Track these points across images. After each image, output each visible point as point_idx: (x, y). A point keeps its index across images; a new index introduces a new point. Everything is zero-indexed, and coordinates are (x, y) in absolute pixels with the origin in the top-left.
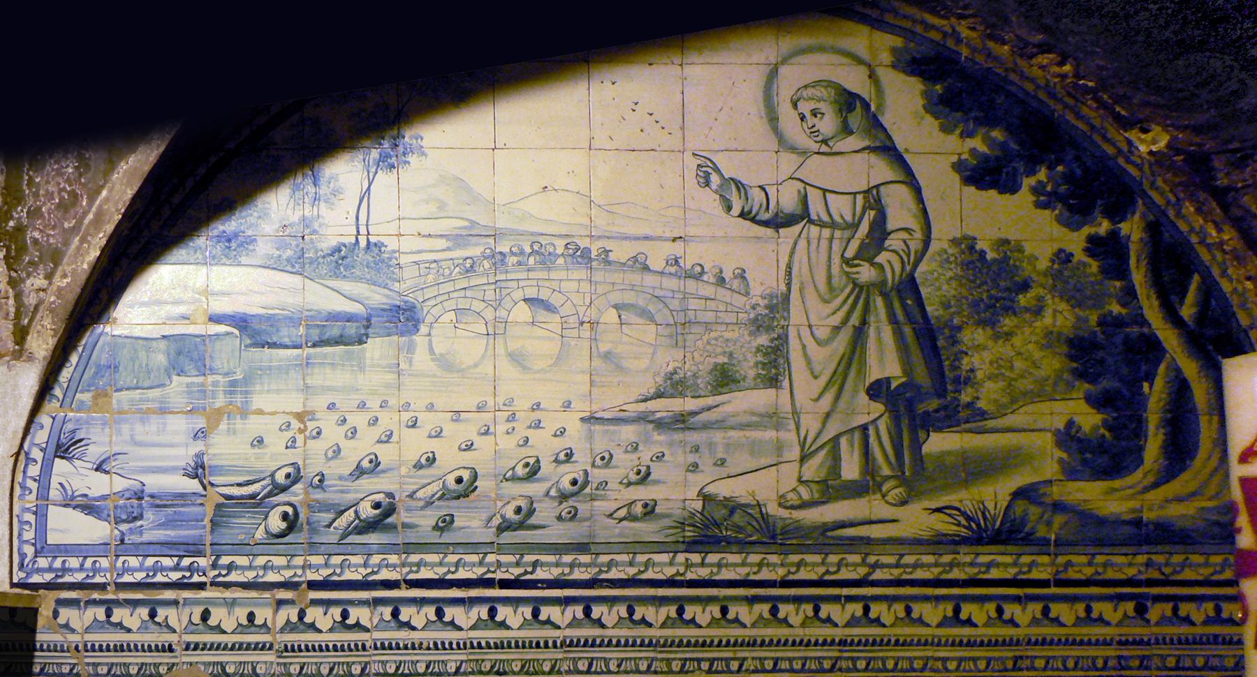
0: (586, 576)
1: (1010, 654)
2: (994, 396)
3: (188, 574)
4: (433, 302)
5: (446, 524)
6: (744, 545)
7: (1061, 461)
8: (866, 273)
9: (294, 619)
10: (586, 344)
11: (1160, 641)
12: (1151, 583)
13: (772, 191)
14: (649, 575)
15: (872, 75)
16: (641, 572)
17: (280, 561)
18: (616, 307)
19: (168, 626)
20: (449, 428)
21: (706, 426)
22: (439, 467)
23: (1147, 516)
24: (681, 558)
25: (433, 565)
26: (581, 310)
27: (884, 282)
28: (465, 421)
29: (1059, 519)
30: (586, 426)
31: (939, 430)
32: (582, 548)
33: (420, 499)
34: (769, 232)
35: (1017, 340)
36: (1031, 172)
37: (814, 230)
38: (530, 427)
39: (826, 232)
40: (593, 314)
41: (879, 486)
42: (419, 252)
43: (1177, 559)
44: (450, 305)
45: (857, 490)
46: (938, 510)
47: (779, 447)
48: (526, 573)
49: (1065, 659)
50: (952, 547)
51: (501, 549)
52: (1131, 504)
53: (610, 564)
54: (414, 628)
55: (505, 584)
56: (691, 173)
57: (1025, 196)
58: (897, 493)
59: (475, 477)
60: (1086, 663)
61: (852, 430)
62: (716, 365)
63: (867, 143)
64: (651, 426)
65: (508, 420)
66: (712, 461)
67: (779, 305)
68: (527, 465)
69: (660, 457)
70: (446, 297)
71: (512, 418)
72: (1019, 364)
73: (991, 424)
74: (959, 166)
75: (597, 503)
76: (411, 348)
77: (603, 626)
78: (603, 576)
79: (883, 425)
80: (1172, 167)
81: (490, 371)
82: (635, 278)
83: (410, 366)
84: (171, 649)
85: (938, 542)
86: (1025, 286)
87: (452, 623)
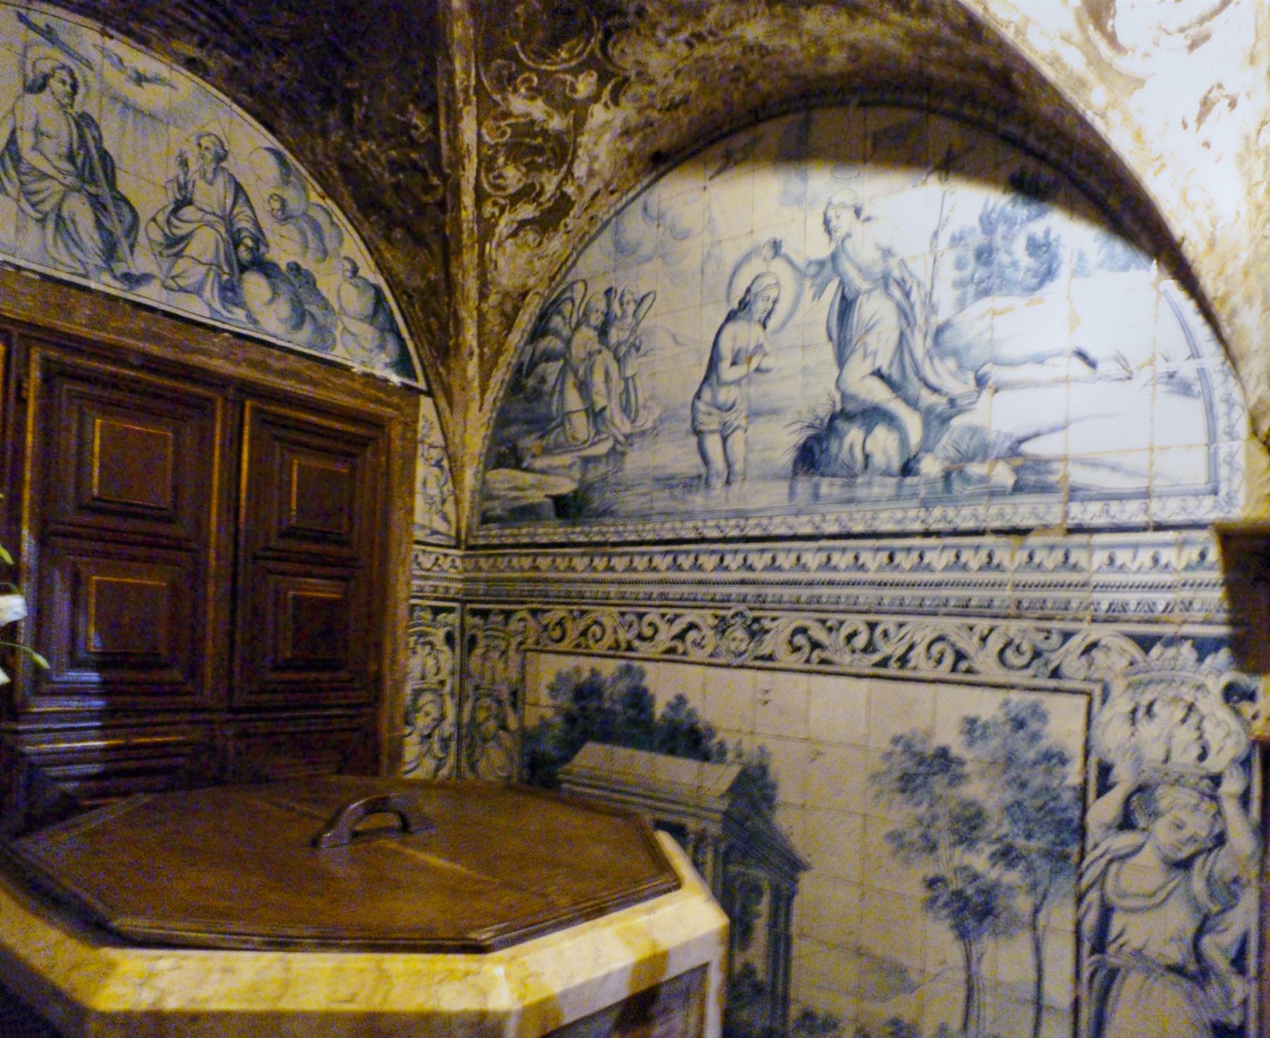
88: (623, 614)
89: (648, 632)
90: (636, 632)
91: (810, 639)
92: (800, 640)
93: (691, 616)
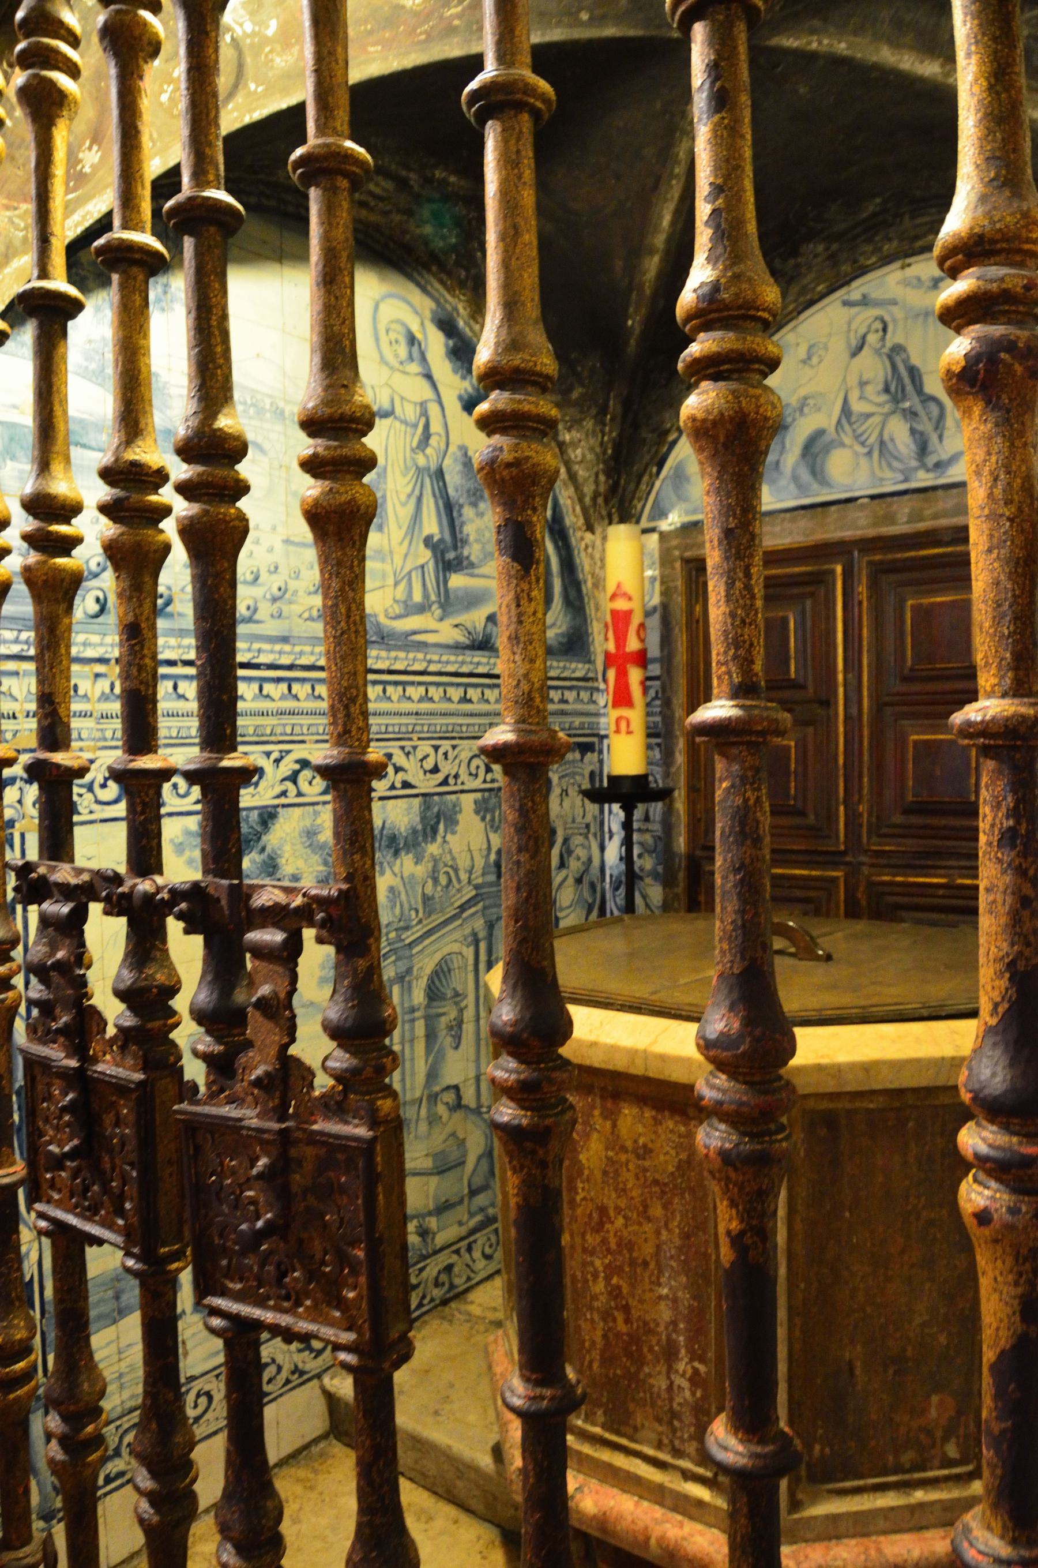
3: (25, 647)
8: (421, 461)
9: (107, 690)
13: (377, 390)
15: (422, 324)
17: (95, 639)
19: (11, 695)
27: (429, 469)
31: (455, 572)
32: (285, 640)
37: (397, 424)
39: (403, 427)
41: (430, 607)
45: (422, 609)
46: (456, 626)
47: (384, 576)
53: (301, 653)
58: (438, 612)
73: (476, 571)
74: (460, 398)
78: (298, 662)
79: (431, 565)
84: (14, 717)
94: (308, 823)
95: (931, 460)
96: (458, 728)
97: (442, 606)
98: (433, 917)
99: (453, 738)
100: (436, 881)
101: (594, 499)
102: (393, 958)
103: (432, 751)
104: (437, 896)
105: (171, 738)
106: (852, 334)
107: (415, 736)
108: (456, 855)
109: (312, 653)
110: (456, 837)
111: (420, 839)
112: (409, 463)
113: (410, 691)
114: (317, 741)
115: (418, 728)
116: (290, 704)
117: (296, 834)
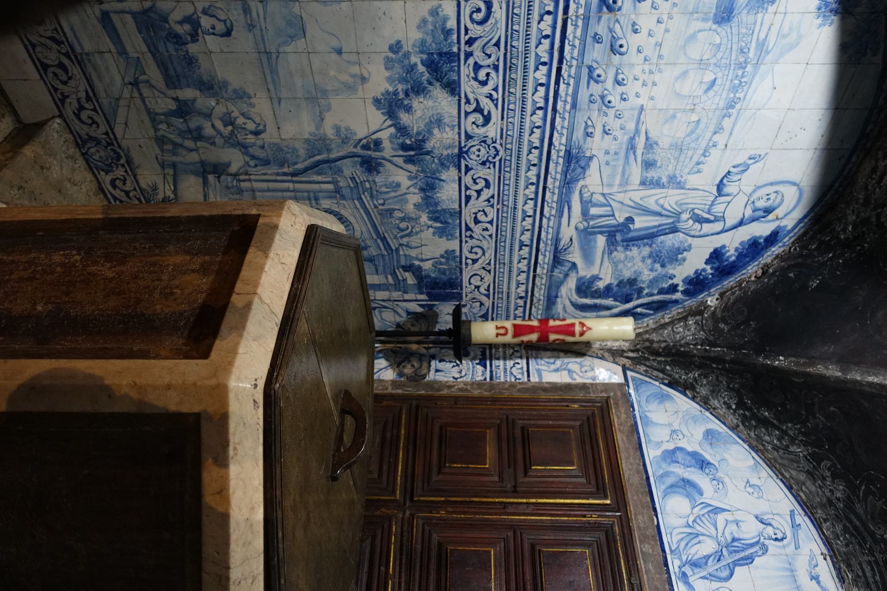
0: (559, 107)
1: (506, 261)
2: (618, 257)
4: (729, 31)
5: (597, 39)
6: (565, 173)
7: (586, 276)
8: (685, 216)
10: (683, 107)
11: (508, 302)
12: (532, 301)
14: (555, 134)
16: (558, 131)
18: (699, 121)
20: (652, 41)
21: (627, 157)
22: (631, 35)
23: (559, 300)
24: (563, 148)
25: (574, 33)
26: (702, 105)
27: (679, 222)
28: (655, 49)
29: (561, 276)
30: (639, 107)
31: (607, 240)
32: (574, 105)
33: (614, 25)
34: (717, 181)
35: (641, 264)
36: (711, 268)
37: (712, 199)
38: (644, 81)
39: (709, 203)
40: (698, 109)
41: (586, 220)
42: (762, 24)
43: (541, 307)
44: (725, 40)
45: (585, 214)
46: (571, 240)
47: (610, 185)
48: (564, 80)
49: (503, 277)
50: (554, 244)
51: (579, 67)
52: (564, 295)
53: (563, 118)
54: (539, 23)
55: (559, 70)
56: (758, 152)
57: (701, 265)
58: (581, 226)
59: (621, 54)
60: (501, 283)
61: (613, 211)
62: (657, 162)
63: (746, 216)
64: (632, 135)
65: (650, 70)
66: (609, 160)
67: (680, 186)
68: (623, 80)
69: (615, 139)
70: (730, 38)
71: (651, 72)
72: (630, 264)
73: (606, 256)
74: (724, 247)
75: (596, 112)
76: (705, 20)
77: (532, 115)
78: (558, 115)
79: (614, 222)
80: (699, 306)
81: (680, 62)
82: (712, 128)
83: (695, 20)
85: (557, 240)
86: (663, 266)
87: (540, 43)
88: (497, 44)
89: (482, 75)
90: (481, 63)
91: (482, 190)
92: (482, 184)
93: (496, 115)
94: (447, 120)
95: (687, 570)
96: (503, 240)
97: (585, 229)
98: (378, 217)
99: (497, 236)
100: (403, 219)
101: (648, 340)
102: (352, 185)
103: (489, 219)
104: (393, 220)
105: (513, 8)
106: (771, 516)
107: (500, 206)
108: (419, 235)
109: (562, 127)
110: (431, 236)
111: (431, 209)
112: (684, 207)
113: (531, 203)
114: (502, 130)
115: (505, 209)
116: (529, 108)
117: (439, 111)
